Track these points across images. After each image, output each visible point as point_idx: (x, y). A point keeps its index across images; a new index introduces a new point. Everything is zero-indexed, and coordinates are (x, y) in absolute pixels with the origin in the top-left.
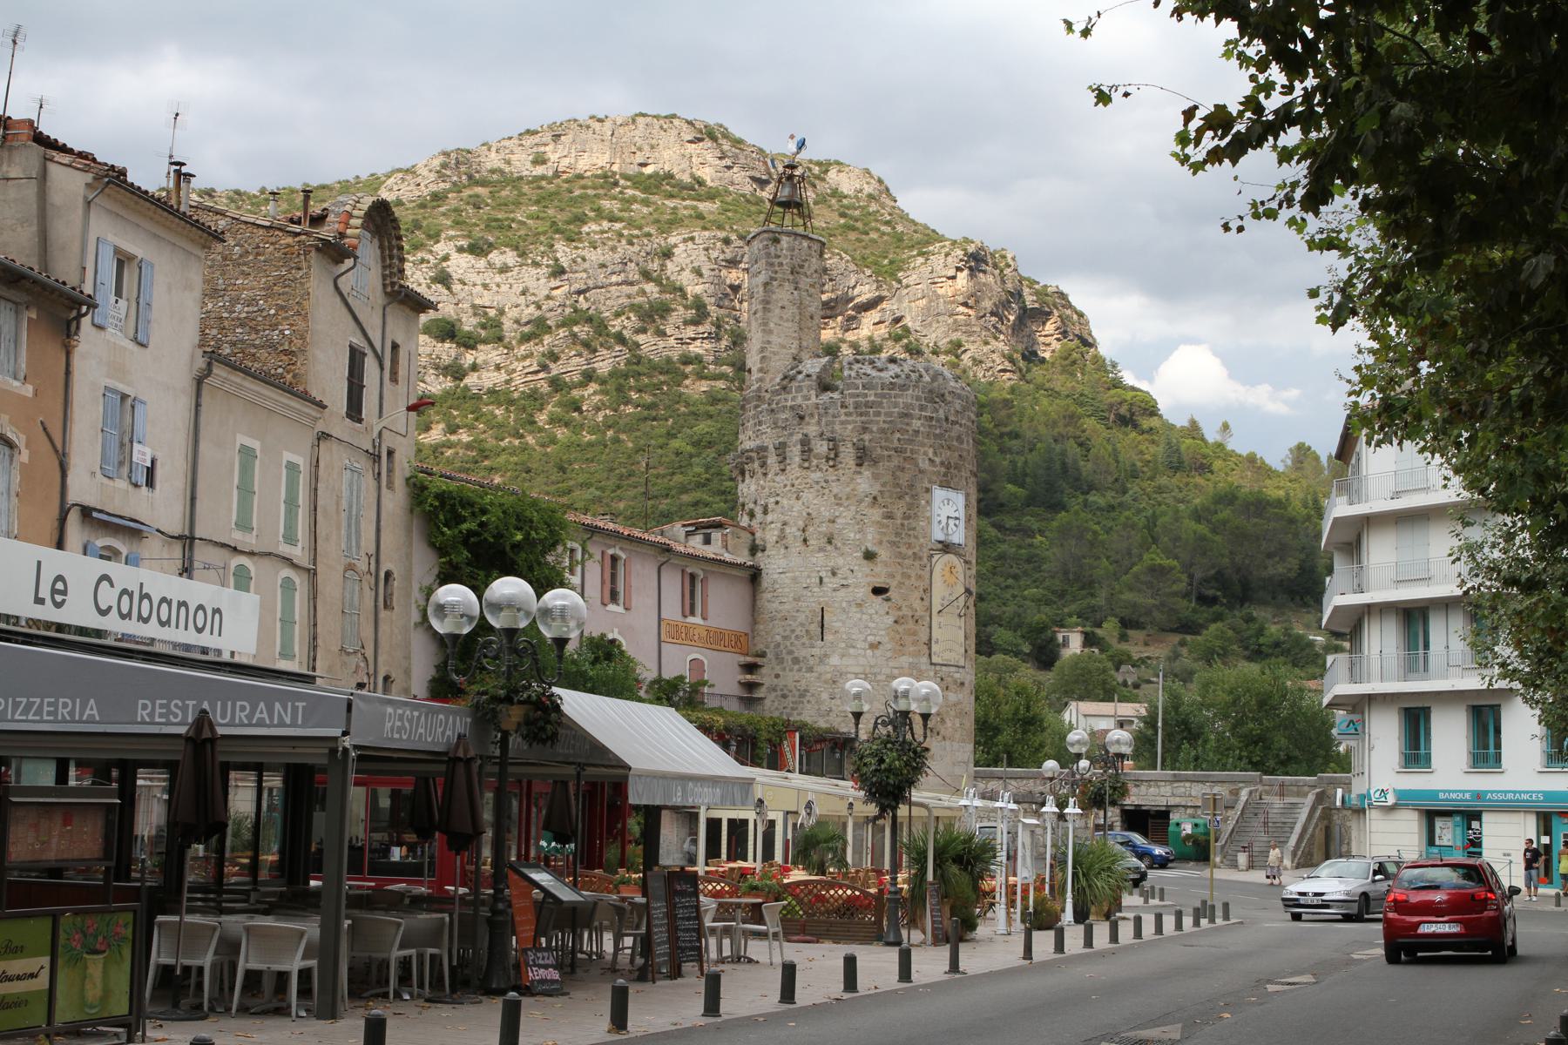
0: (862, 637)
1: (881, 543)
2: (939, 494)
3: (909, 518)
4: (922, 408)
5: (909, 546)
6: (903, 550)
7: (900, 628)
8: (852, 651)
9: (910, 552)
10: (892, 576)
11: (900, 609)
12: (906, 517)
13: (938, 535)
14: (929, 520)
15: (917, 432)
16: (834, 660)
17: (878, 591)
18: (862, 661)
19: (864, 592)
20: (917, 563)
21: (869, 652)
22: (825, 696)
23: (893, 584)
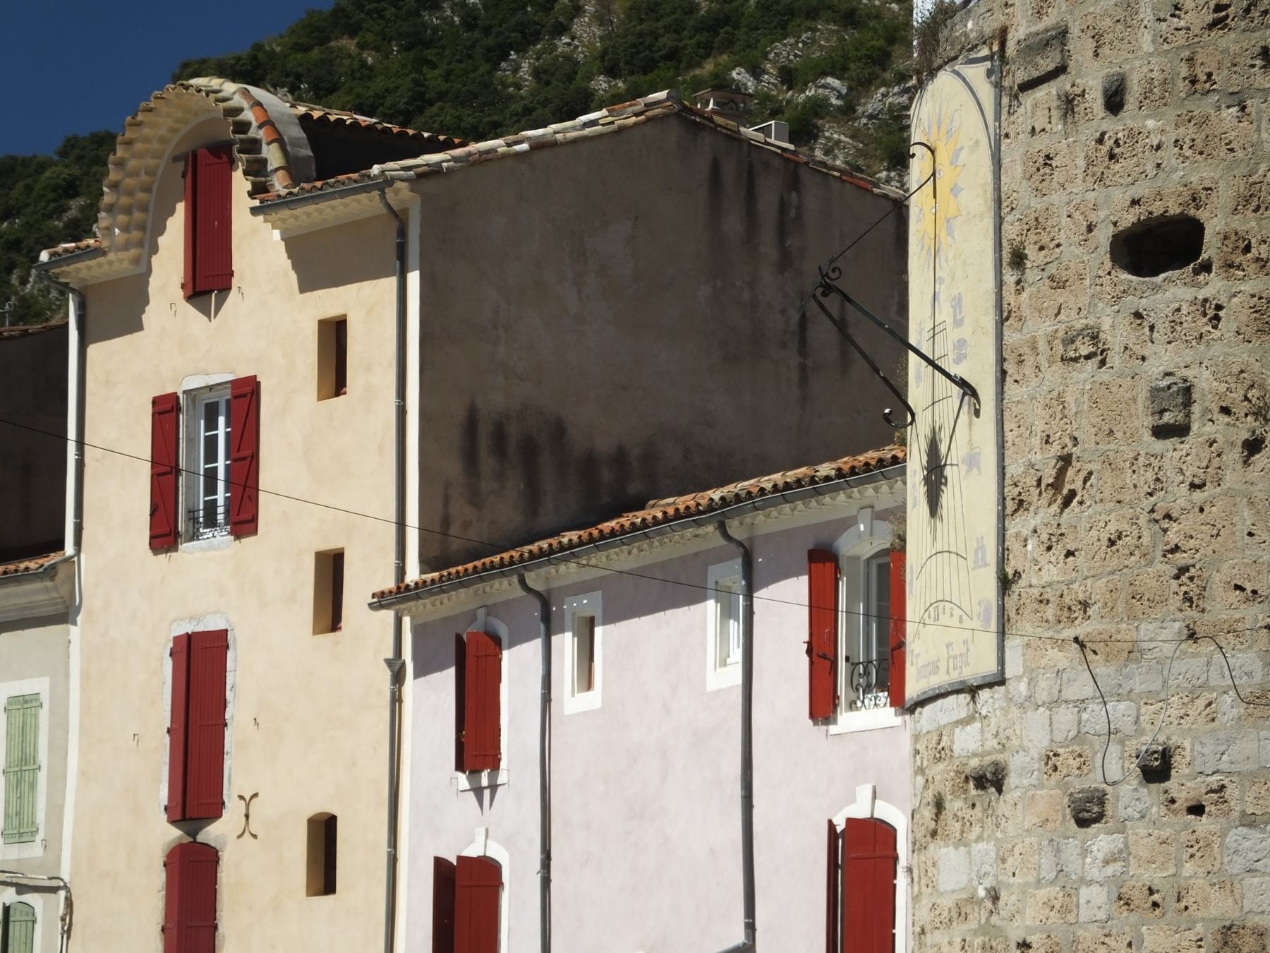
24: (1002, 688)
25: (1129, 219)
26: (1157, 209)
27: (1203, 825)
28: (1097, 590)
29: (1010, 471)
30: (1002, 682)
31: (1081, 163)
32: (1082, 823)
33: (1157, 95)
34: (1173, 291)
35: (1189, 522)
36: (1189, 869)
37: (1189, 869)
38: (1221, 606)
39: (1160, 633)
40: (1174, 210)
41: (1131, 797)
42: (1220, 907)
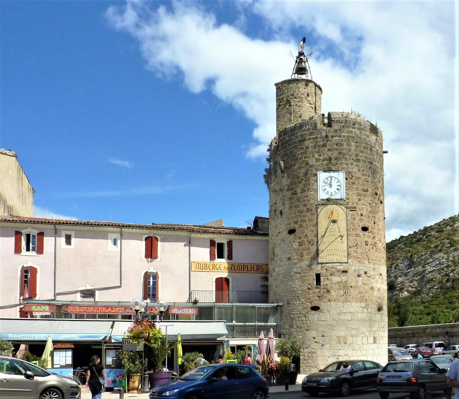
0: (284, 256)
1: (291, 207)
2: (322, 176)
3: (305, 191)
4: (311, 134)
5: (305, 205)
6: (301, 208)
7: (301, 248)
8: (282, 263)
9: (305, 208)
10: (296, 223)
11: (300, 238)
12: (303, 191)
13: (322, 196)
14: (316, 190)
15: (307, 148)
16: (277, 270)
17: (292, 232)
18: (285, 267)
19: (285, 233)
20: (309, 214)
21: (287, 262)
22: (274, 287)
23: (296, 226)
24: (348, 264)
25: (363, 226)
26: (366, 226)
27: (370, 278)
28: (360, 257)
29: (349, 244)
30: (348, 263)
31: (358, 220)
32: (358, 276)
33: (365, 216)
34: (366, 233)
35: (368, 253)
36: (369, 282)
37: (369, 282)
38: (371, 261)
39: (366, 262)
40: (367, 227)
41: (364, 275)
42: (371, 285)
